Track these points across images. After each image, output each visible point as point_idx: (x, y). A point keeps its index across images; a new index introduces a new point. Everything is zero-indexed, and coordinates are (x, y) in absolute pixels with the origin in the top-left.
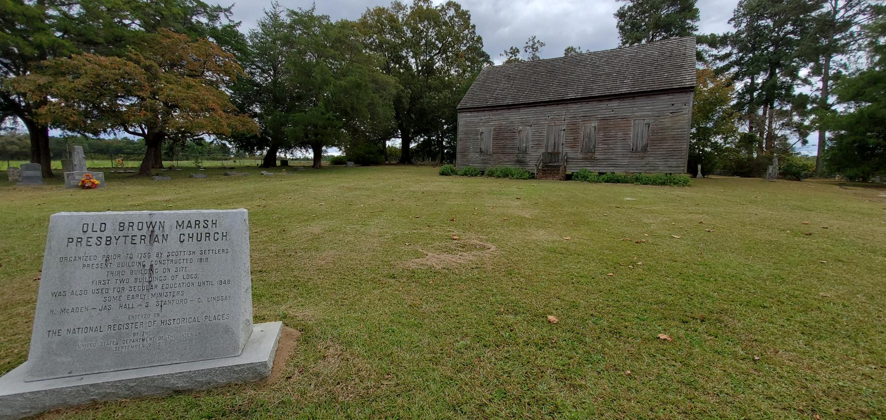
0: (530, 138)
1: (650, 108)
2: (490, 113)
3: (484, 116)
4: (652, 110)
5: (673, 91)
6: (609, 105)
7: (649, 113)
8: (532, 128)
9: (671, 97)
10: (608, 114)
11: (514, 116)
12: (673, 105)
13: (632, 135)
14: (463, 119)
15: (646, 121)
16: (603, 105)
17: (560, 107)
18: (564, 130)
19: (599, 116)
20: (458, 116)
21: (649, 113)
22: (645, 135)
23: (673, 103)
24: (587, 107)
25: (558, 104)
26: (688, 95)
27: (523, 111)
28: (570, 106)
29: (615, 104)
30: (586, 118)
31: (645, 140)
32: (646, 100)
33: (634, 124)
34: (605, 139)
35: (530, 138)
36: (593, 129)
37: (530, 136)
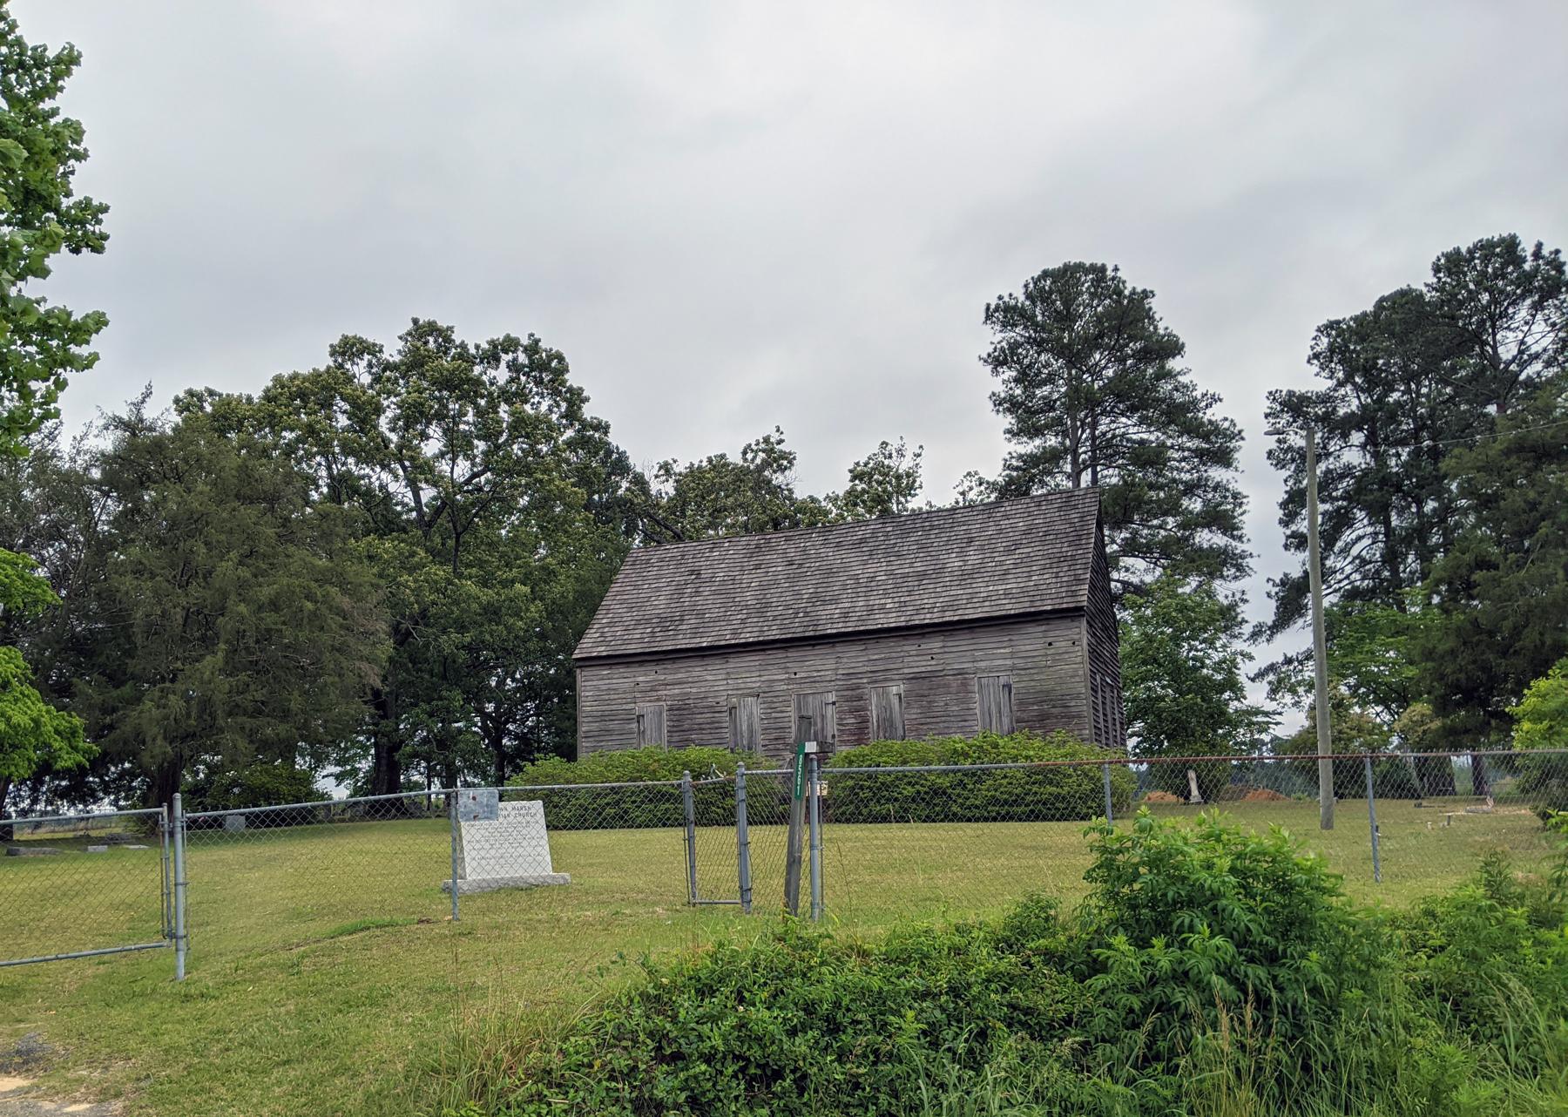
0: (757, 726)
1: (1007, 650)
2: (656, 668)
3: (644, 676)
4: (1012, 656)
5: (1045, 616)
6: (923, 647)
7: (1008, 662)
8: (760, 700)
9: (1043, 628)
10: (923, 665)
11: (712, 680)
12: (1050, 644)
13: (977, 711)
14: (591, 688)
15: (1002, 681)
16: (910, 647)
17: (819, 650)
18: (834, 703)
19: (906, 671)
20: (579, 677)
21: (1008, 662)
22: (1005, 710)
23: (1049, 640)
24: (877, 653)
25: (814, 645)
26: (1076, 624)
27: (735, 663)
28: (839, 648)
29: (935, 644)
30: (879, 678)
31: (1006, 721)
32: (968, 636)
33: (981, 686)
34: (923, 721)
35: (757, 726)
36: (896, 701)
37: (756, 720)
